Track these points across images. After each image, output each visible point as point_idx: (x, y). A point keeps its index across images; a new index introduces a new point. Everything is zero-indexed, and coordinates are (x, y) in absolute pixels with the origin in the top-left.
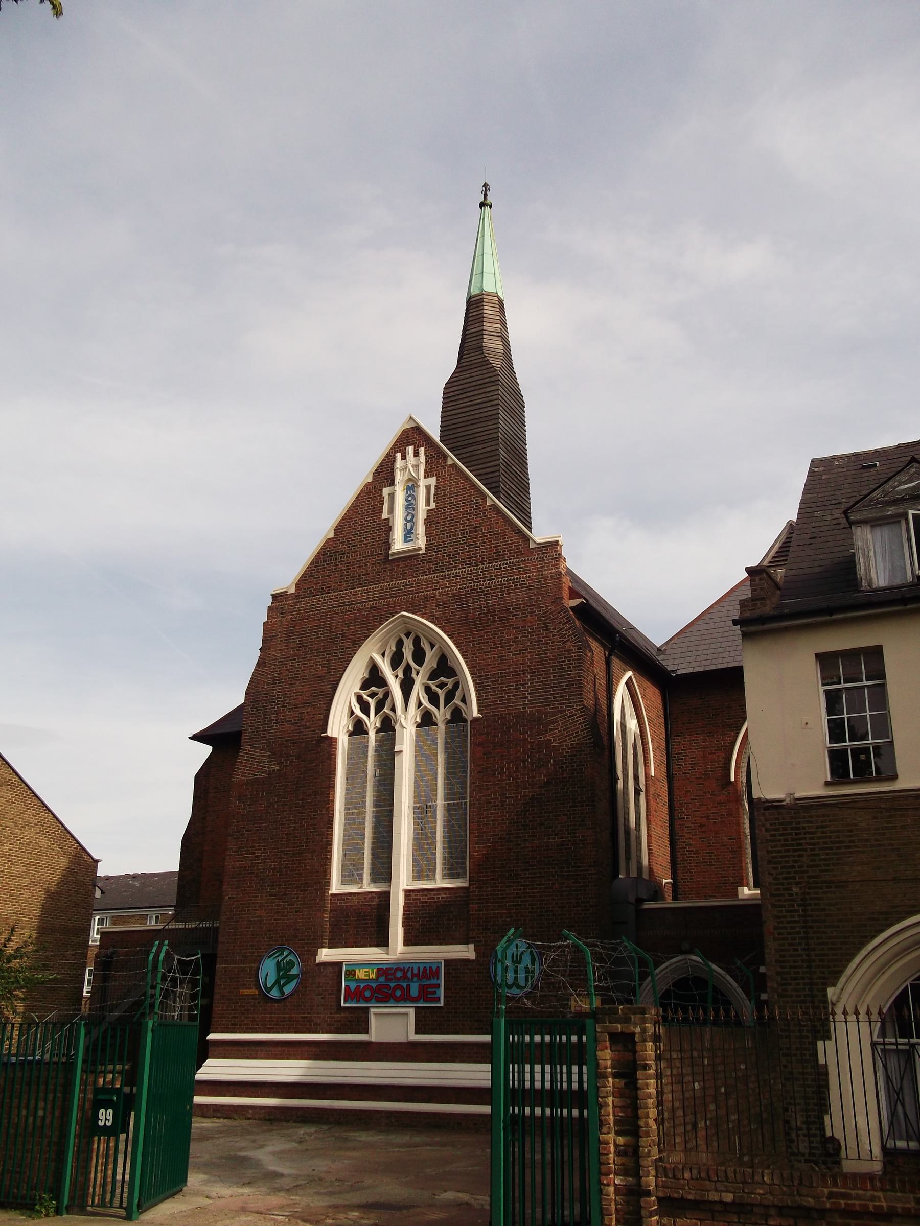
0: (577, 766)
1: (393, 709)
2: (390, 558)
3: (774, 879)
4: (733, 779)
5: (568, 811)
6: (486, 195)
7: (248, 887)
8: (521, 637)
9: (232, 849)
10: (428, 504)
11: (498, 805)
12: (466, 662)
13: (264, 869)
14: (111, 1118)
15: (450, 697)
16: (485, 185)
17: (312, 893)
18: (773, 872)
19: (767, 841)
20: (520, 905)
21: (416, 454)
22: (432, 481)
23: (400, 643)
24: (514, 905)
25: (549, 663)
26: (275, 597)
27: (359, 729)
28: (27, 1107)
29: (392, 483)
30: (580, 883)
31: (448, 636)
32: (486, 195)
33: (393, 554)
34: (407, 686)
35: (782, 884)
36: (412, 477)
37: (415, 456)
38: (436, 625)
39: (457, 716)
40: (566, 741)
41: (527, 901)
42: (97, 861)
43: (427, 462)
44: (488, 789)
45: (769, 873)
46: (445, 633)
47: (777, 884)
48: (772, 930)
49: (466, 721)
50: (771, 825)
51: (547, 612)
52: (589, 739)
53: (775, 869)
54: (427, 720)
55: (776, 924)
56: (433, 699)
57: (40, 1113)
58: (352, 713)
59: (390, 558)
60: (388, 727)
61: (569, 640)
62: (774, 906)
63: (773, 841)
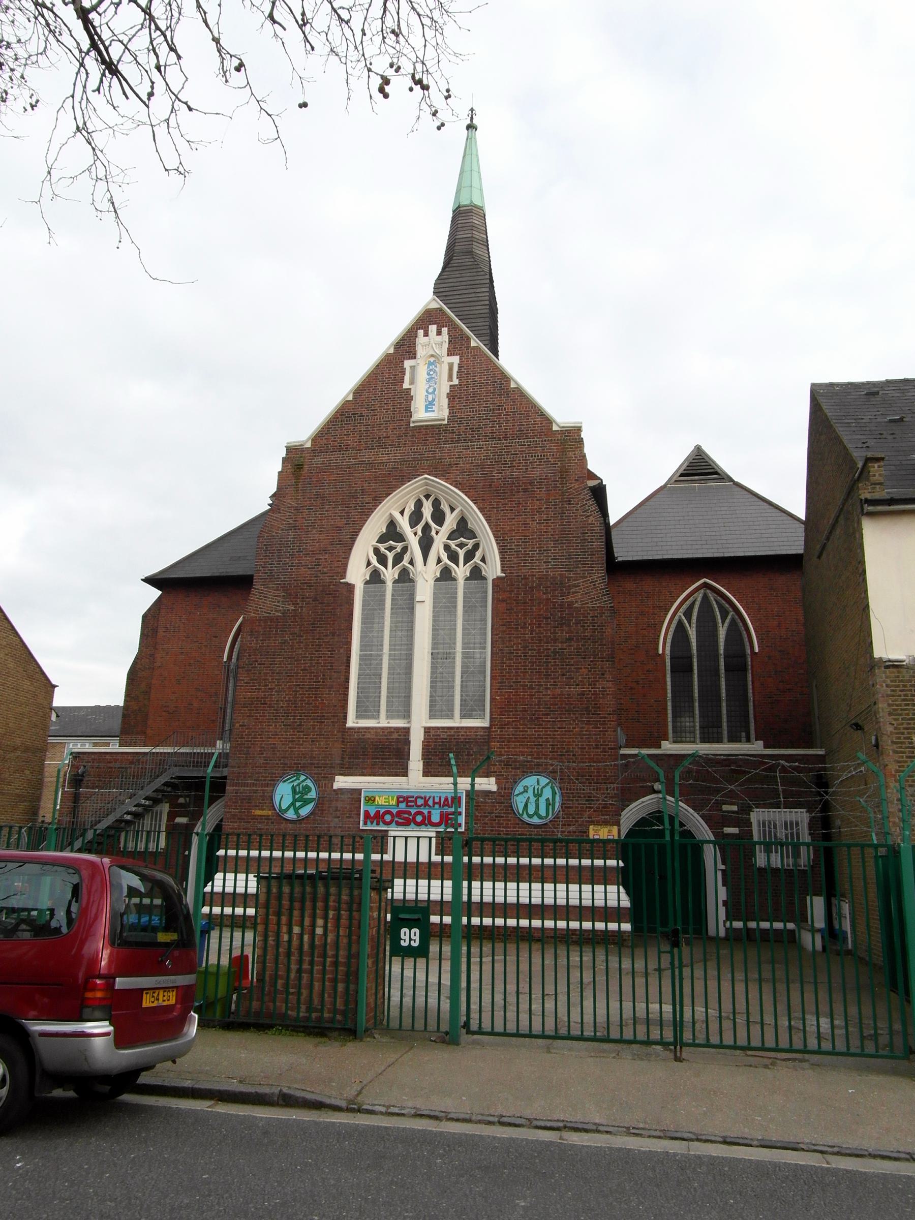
0: (598, 626)
1: (411, 562)
2: (412, 425)
3: (896, 728)
4: (660, 652)
5: (589, 665)
6: (472, 118)
7: (261, 716)
8: (545, 508)
9: (243, 680)
10: (450, 378)
11: (521, 656)
12: (490, 526)
13: (277, 701)
14: (417, 938)
15: (469, 556)
16: (472, 110)
17: (329, 726)
18: (894, 722)
19: (888, 696)
20: (542, 745)
21: (439, 333)
22: (456, 360)
23: (419, 504)
24: (535, 745)
25: (572, 534)
26: (289, 450)
27: (375, 578)
28: (301, 925)
29: (414, 357)
30: (599, 728)
31: (472, 501)
32: (472, 118)
33: (414, 422)
34: (426, 544)
35: (903, 733)
36: (435, 354)
37: (437, 335)
38: (460, 490)
39: (476, 574)
40: (588, 603)
41: (548, 742)
42: (54, 686)
43: (450, 342)
44: (510, 641)
45: (890, 724)
46: (469, 498)
47: (897, 733)
48: (893, 773)
49: (485, 578)
50: (892, 681)
51: (571, 488)
52: (610, 603)
53: (895, 719)
54: (446, 575)
55: (897, 768)
56: (453, 557)
57: (319, 931)
58: (369, 564)
59: (412, 425)
60: (405, 578)
61: (591, 515)
62: (895, 752)
63: (893, 696)
